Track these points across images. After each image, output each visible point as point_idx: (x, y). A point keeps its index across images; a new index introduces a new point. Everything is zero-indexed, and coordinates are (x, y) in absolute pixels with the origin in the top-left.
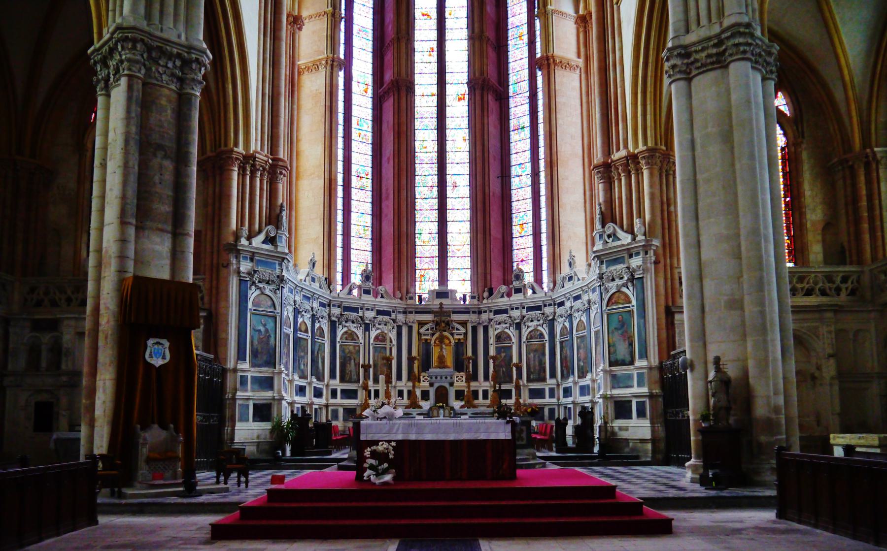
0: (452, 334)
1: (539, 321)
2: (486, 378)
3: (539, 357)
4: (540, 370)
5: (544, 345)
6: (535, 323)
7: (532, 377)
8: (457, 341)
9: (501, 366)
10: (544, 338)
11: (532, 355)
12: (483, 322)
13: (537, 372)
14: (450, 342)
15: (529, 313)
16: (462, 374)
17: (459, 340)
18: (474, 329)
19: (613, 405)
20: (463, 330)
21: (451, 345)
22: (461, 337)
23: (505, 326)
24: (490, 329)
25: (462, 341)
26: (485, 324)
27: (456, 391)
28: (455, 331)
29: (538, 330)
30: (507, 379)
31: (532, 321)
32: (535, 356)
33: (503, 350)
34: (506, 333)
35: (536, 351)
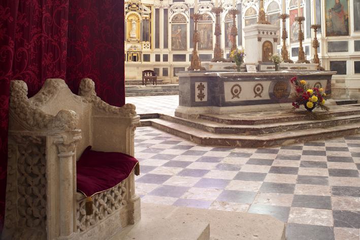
0: (140, 14)
1: (208, 8)
2: (166, 46)
3: (207, 33)
4: (208, 41)
5: (212, 25)
6: (205, 9)
7: (202, 46)
8: (144, 19)
9: (178, 38)
10: (211, 20)
11: (202, 31)
12: (164, 7)
13: (206, 43)
14: (139, 19)
15: (201, 2)
16: (148, 42)
17: (146, 18)
18: (157, 11)
19: (329, 65)
20: (149, 11)
21: (139, 22)
22: (148, 16)
23: (182, 10)
24: (169, 11)
25: (148, 19)
26: (166, 8)
27: (167, 55)
28: (143, 11)
29: (207, 15)
30: (184, 48)
31: (203, 8)
32: (204, 32)
33: (179, 27)
34: (182, 15)
35: (205, 28)
